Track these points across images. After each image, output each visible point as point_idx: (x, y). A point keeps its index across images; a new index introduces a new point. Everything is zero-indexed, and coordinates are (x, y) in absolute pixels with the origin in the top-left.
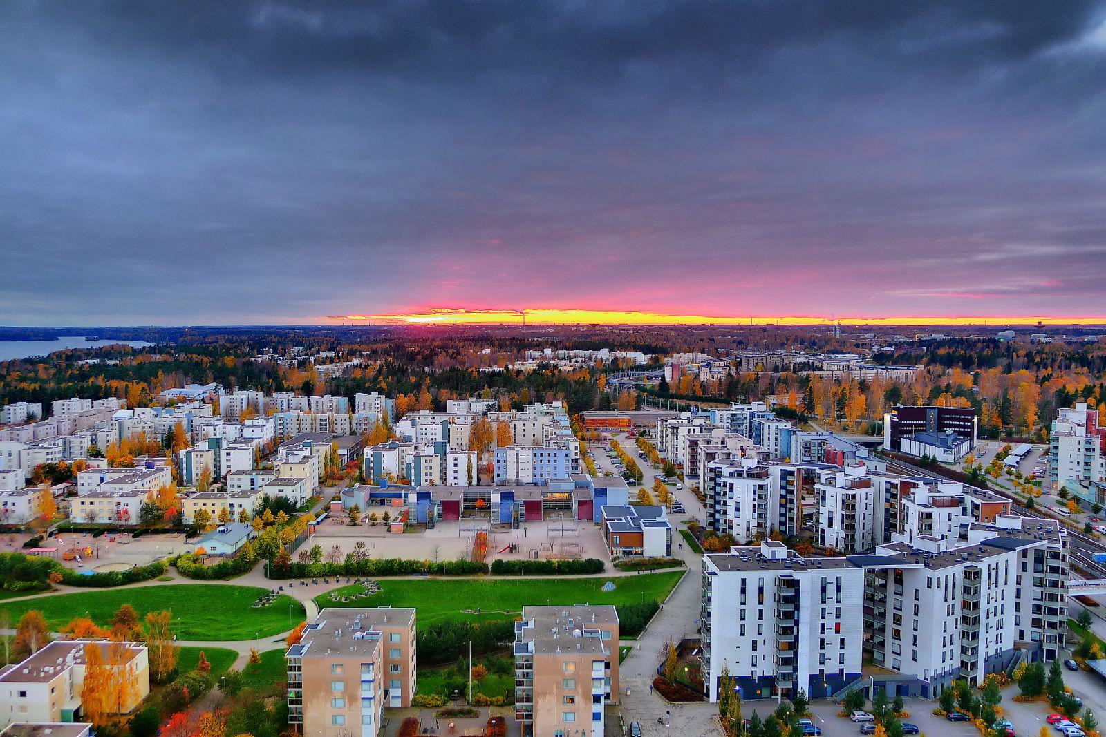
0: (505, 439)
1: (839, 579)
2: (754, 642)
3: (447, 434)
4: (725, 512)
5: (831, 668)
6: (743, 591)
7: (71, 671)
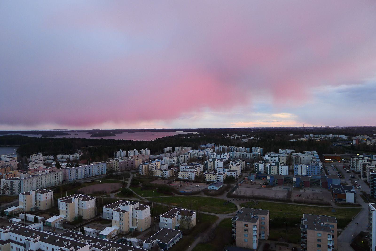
0: (298, 161)
3: (279, 159)
7: (177, 216)
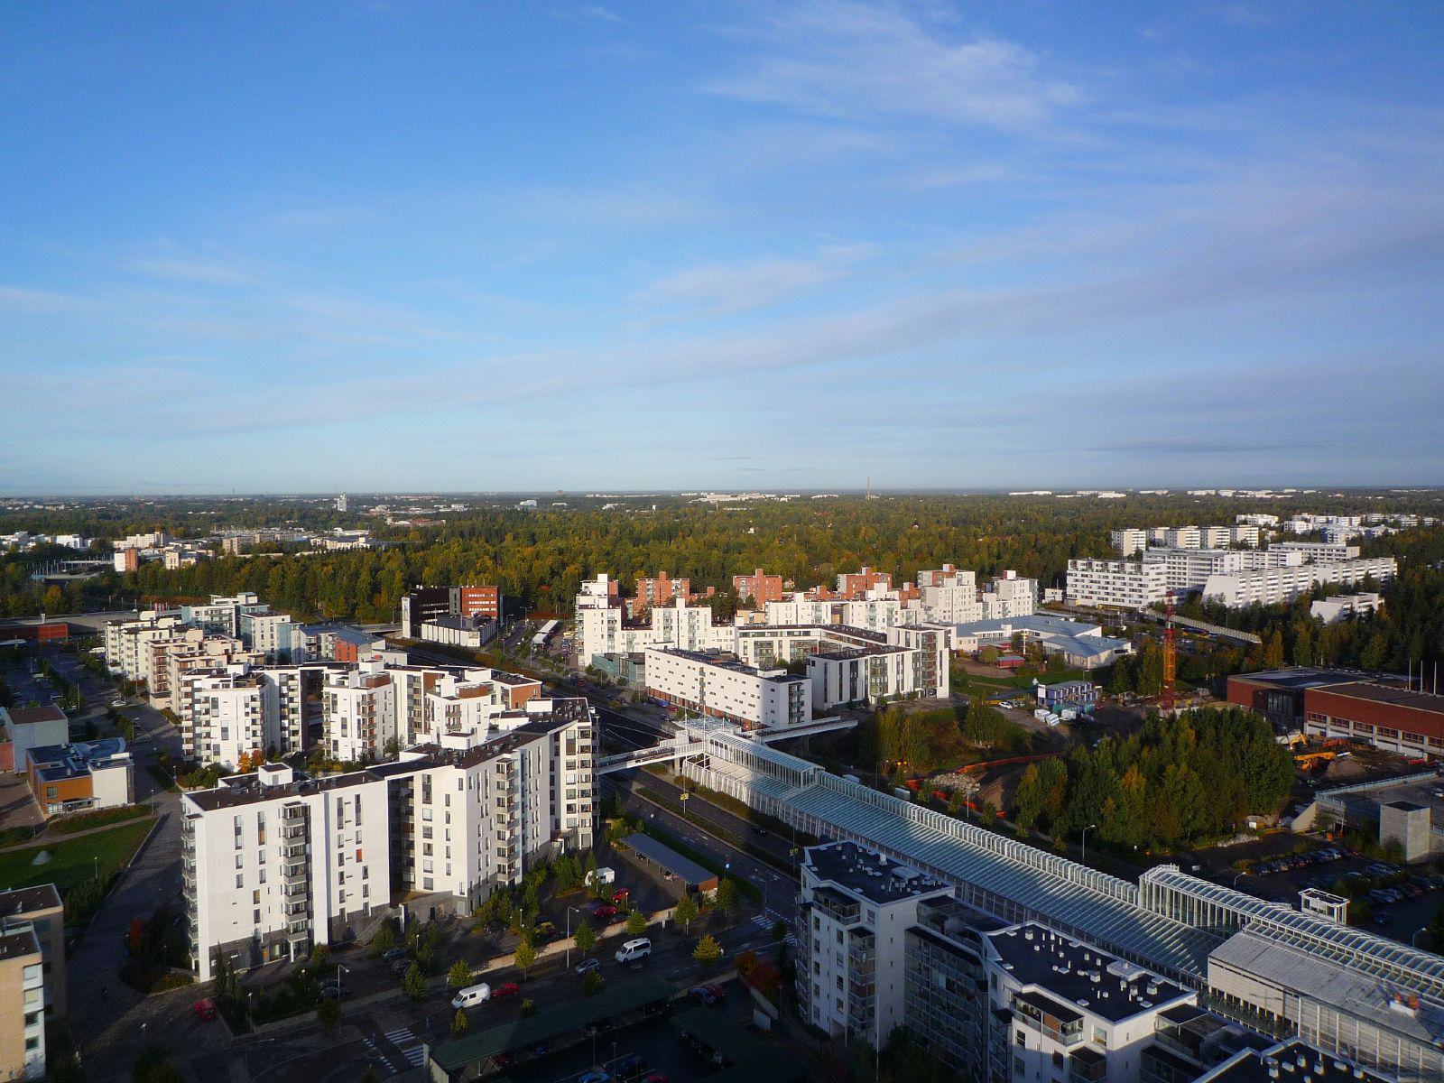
1: (358, 797)
2: (256, 894)
4: (208, 735)
5: (354, 905)
6: (238, 831)
